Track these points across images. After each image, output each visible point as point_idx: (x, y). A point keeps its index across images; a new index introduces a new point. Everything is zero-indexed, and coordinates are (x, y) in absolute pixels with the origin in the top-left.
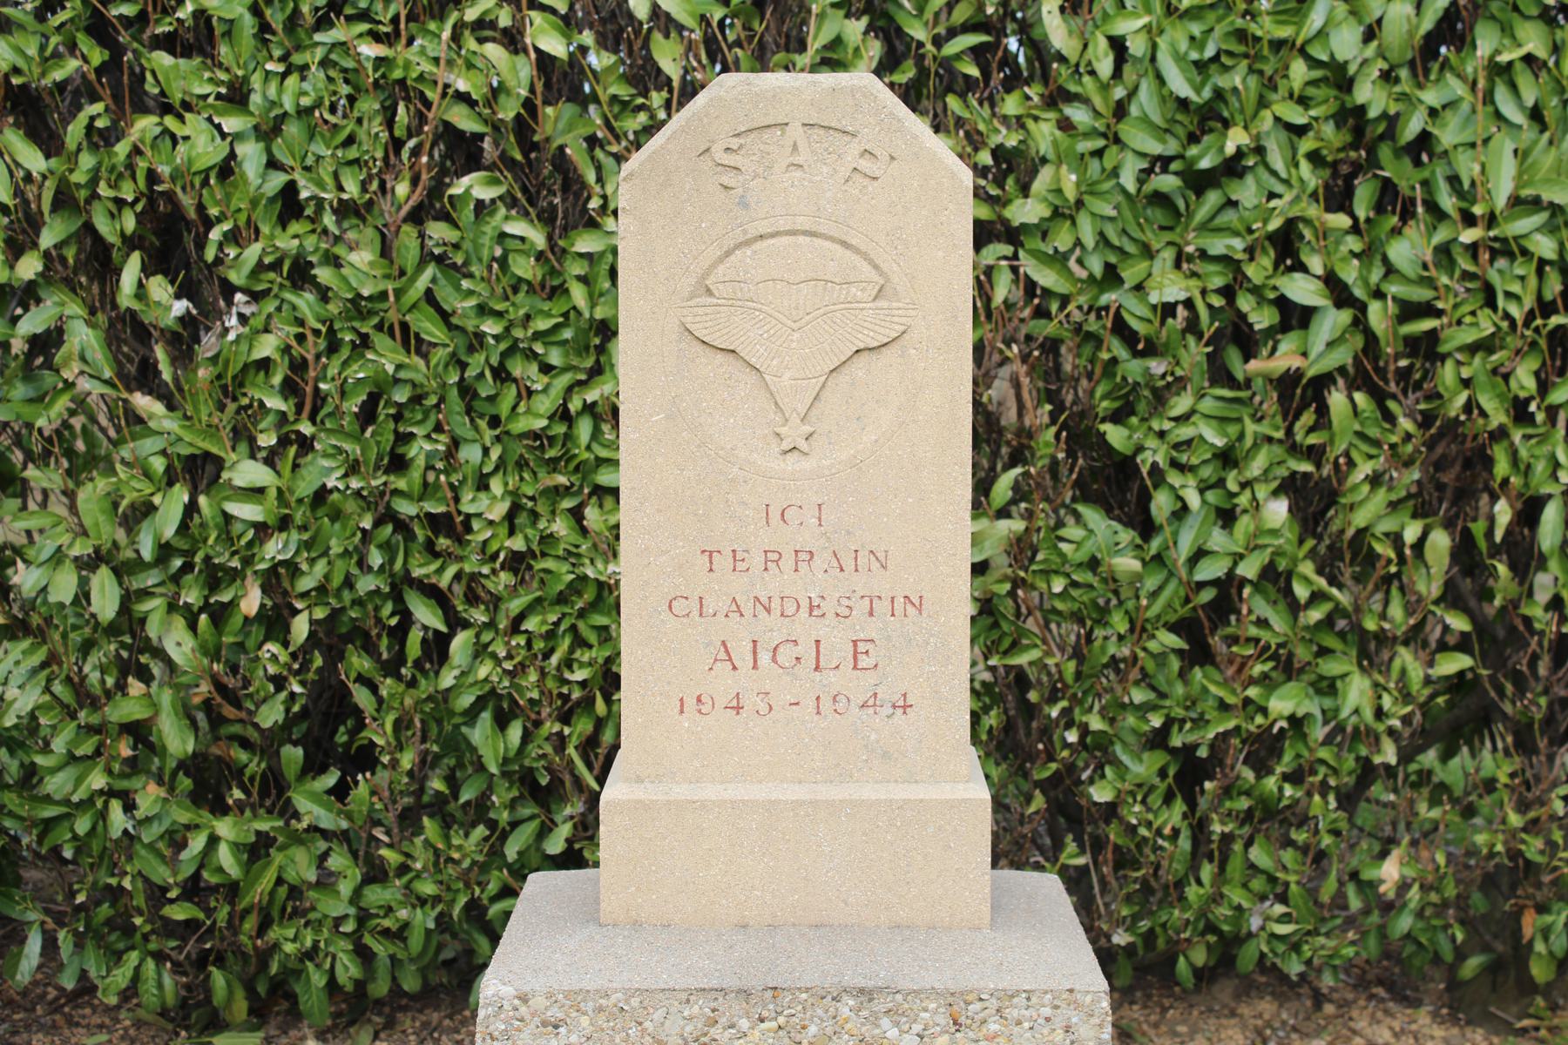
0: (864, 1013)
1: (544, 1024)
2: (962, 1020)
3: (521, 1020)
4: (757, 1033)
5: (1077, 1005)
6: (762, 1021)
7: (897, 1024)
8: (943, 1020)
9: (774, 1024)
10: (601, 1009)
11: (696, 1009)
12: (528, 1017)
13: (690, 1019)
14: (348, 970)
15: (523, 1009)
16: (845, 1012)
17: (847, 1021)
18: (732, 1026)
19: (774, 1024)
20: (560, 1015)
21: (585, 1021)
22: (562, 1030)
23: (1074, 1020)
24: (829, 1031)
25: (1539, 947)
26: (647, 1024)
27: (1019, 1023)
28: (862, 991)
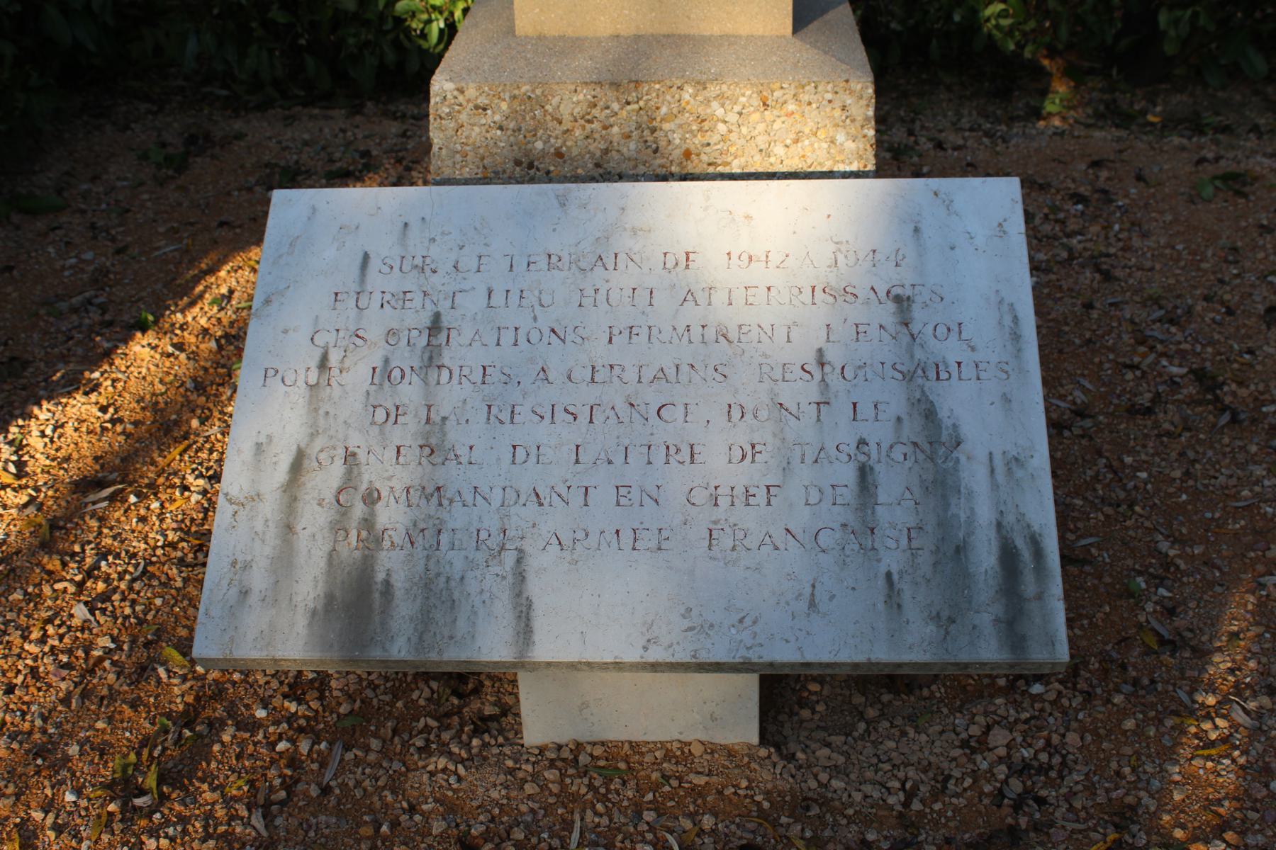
0: (700, 98)
1: (477, 107)
2: (769, 102)
3: (460, 105)
4: (624, 113)
5: (851, 92)
6: (628, 103)
7: (723, 105)
8: (756, 102)
9: (636, 107)
10: (514, 97)
11: (581, 97)
12: (465, 103)
13: (579, 102)
14: (391, 57)
15: (461, 98)
16: (686, 97)
17: (688, 103)
18: (607, 108)
19: (636, 107)
20: (487, 102)
21: (504, 106)
22: (489, 112)
23: (849, 102)
24: (675, 111)
25: (1172, 33)
26: (548, 107)
27: (810, 104)
28: (698, 83)
